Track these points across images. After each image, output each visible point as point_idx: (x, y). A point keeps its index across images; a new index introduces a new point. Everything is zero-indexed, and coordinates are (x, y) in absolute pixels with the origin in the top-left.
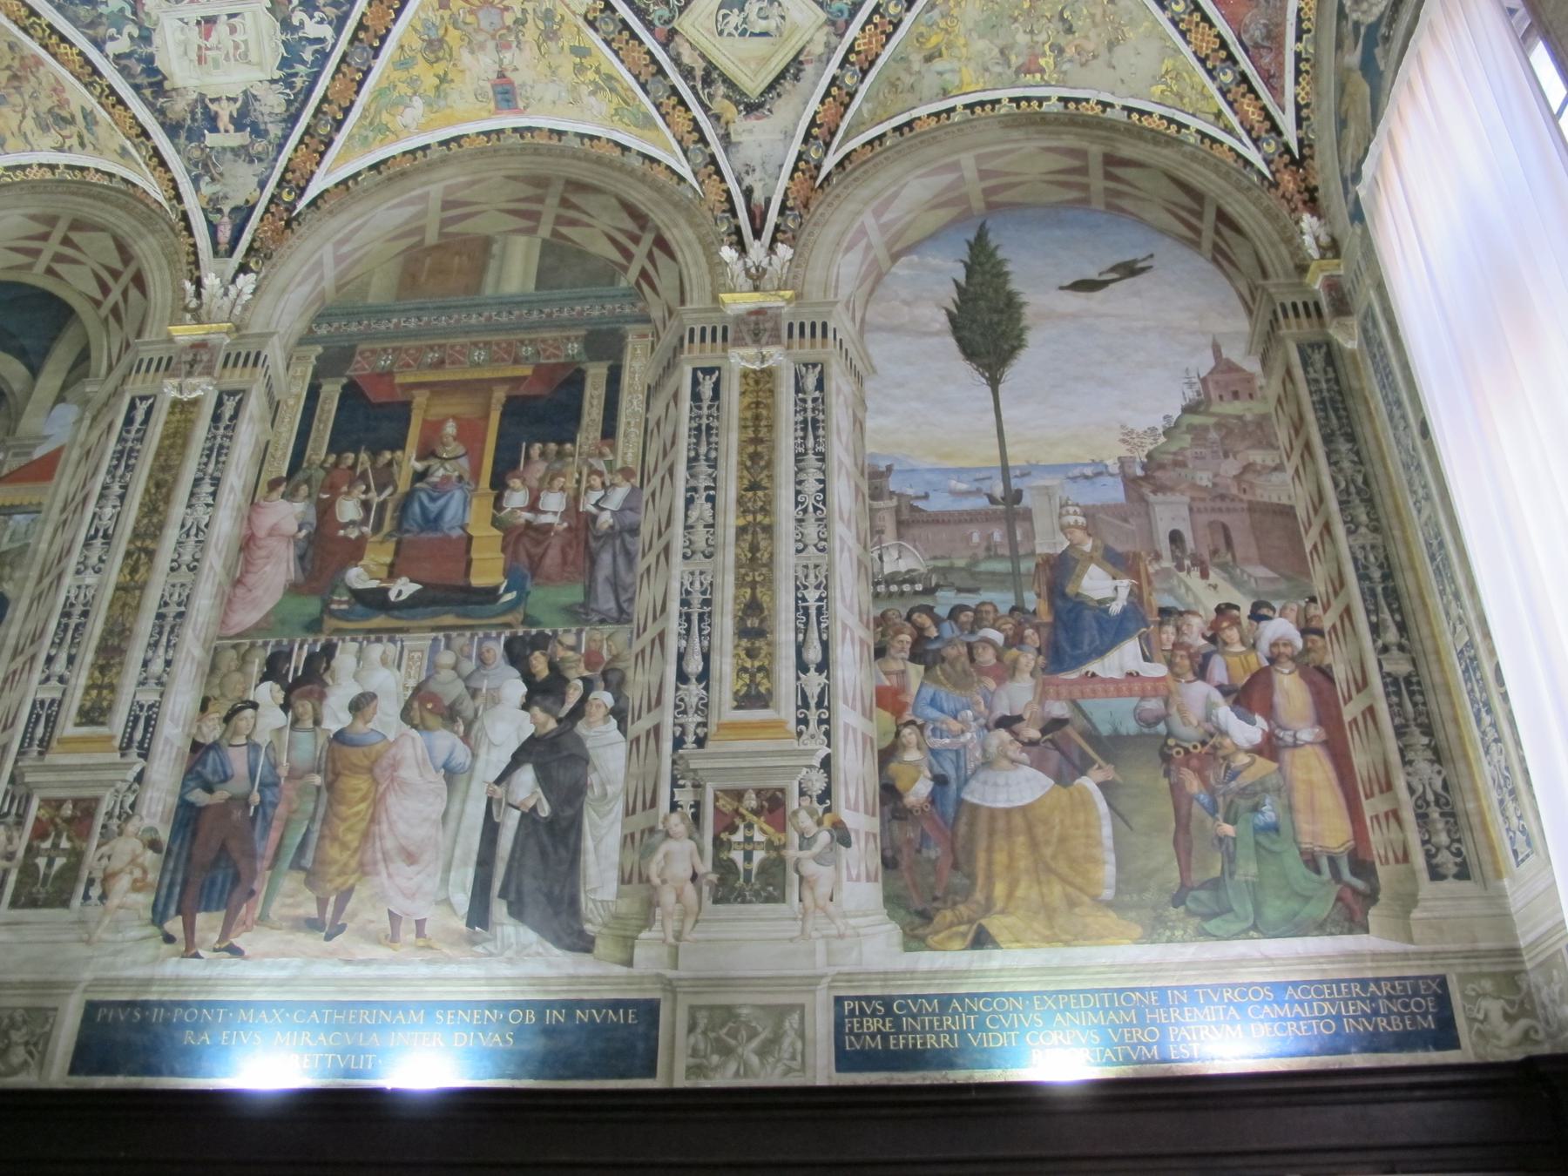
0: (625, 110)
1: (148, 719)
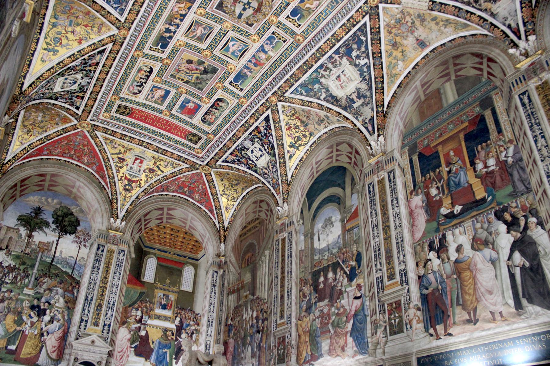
0: (458, 27)
1: (405, 273)
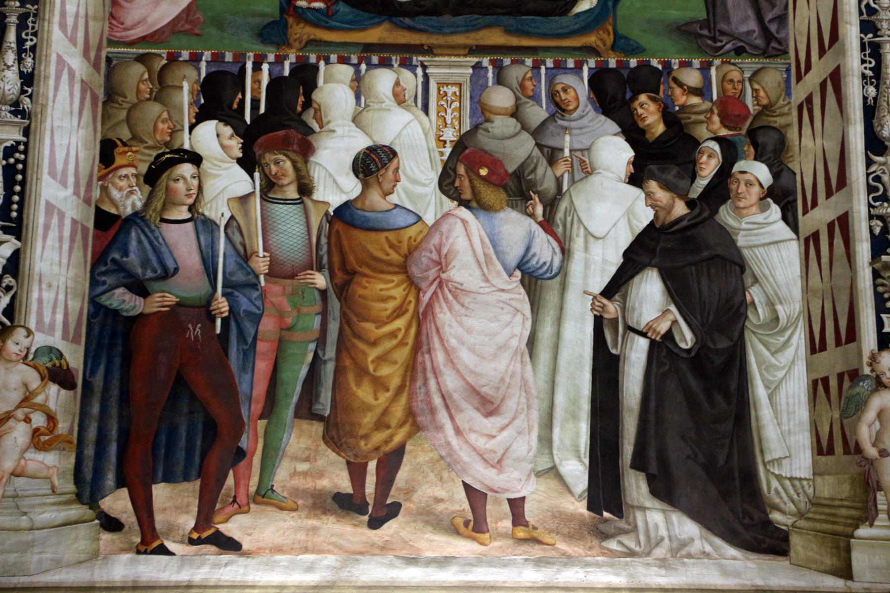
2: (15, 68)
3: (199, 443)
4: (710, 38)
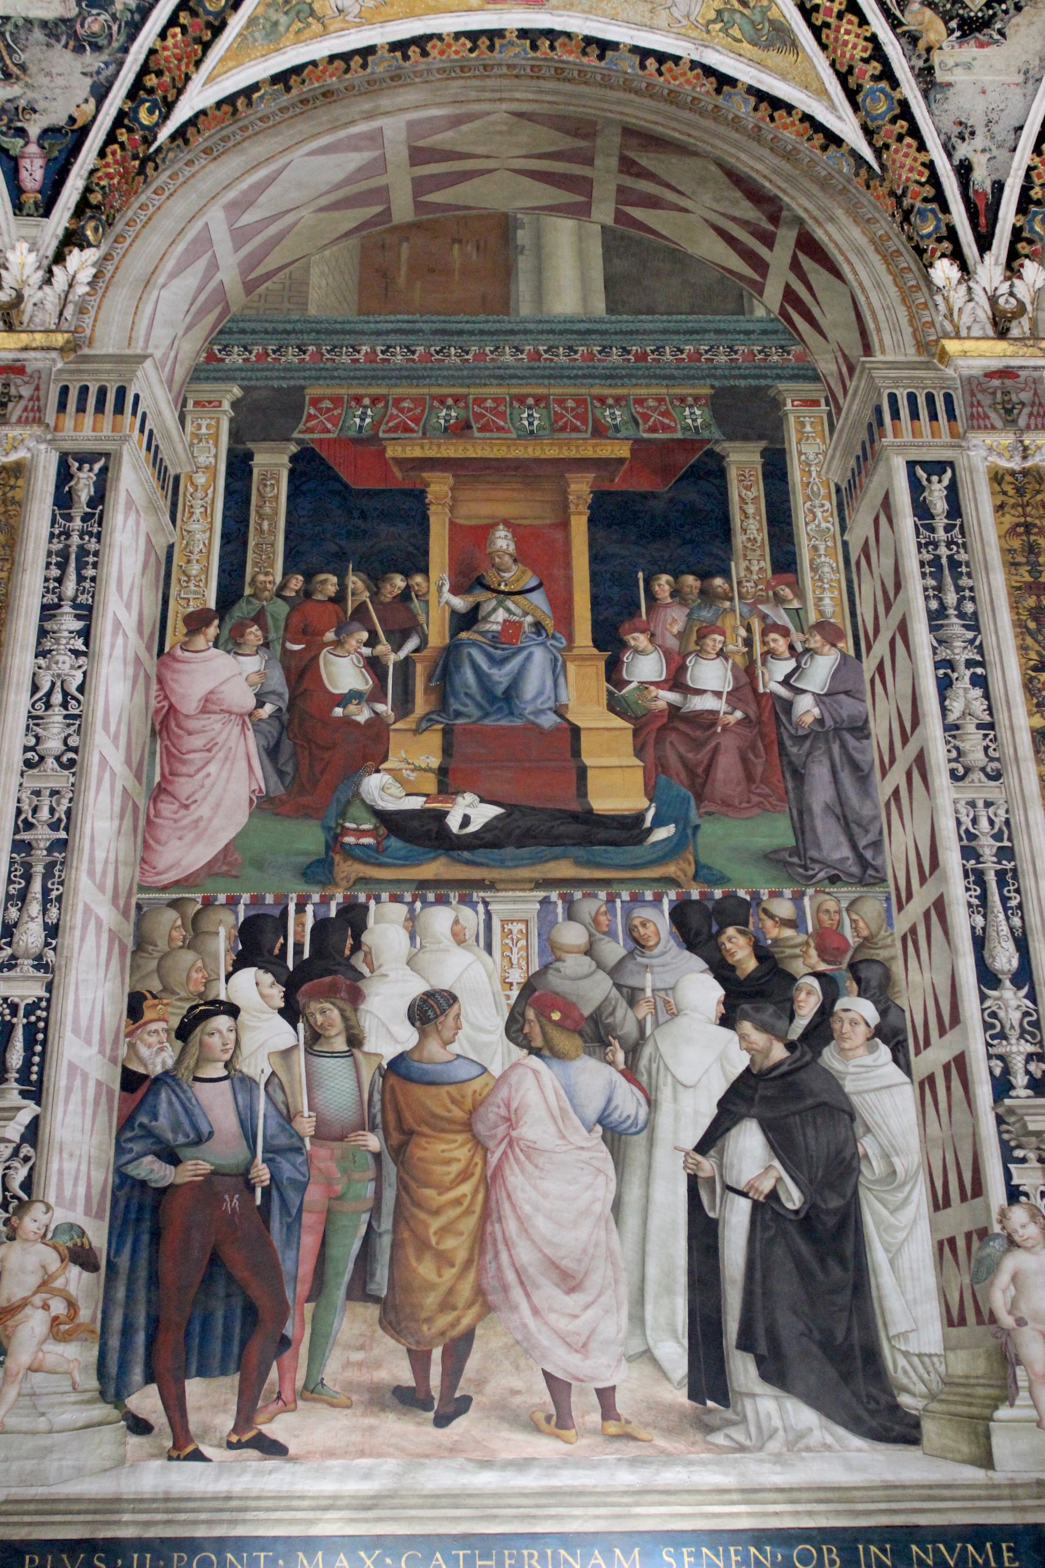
1: (30, 1030)
2: (40, 920)
3: (237, 1330)
4: (801, 866)
